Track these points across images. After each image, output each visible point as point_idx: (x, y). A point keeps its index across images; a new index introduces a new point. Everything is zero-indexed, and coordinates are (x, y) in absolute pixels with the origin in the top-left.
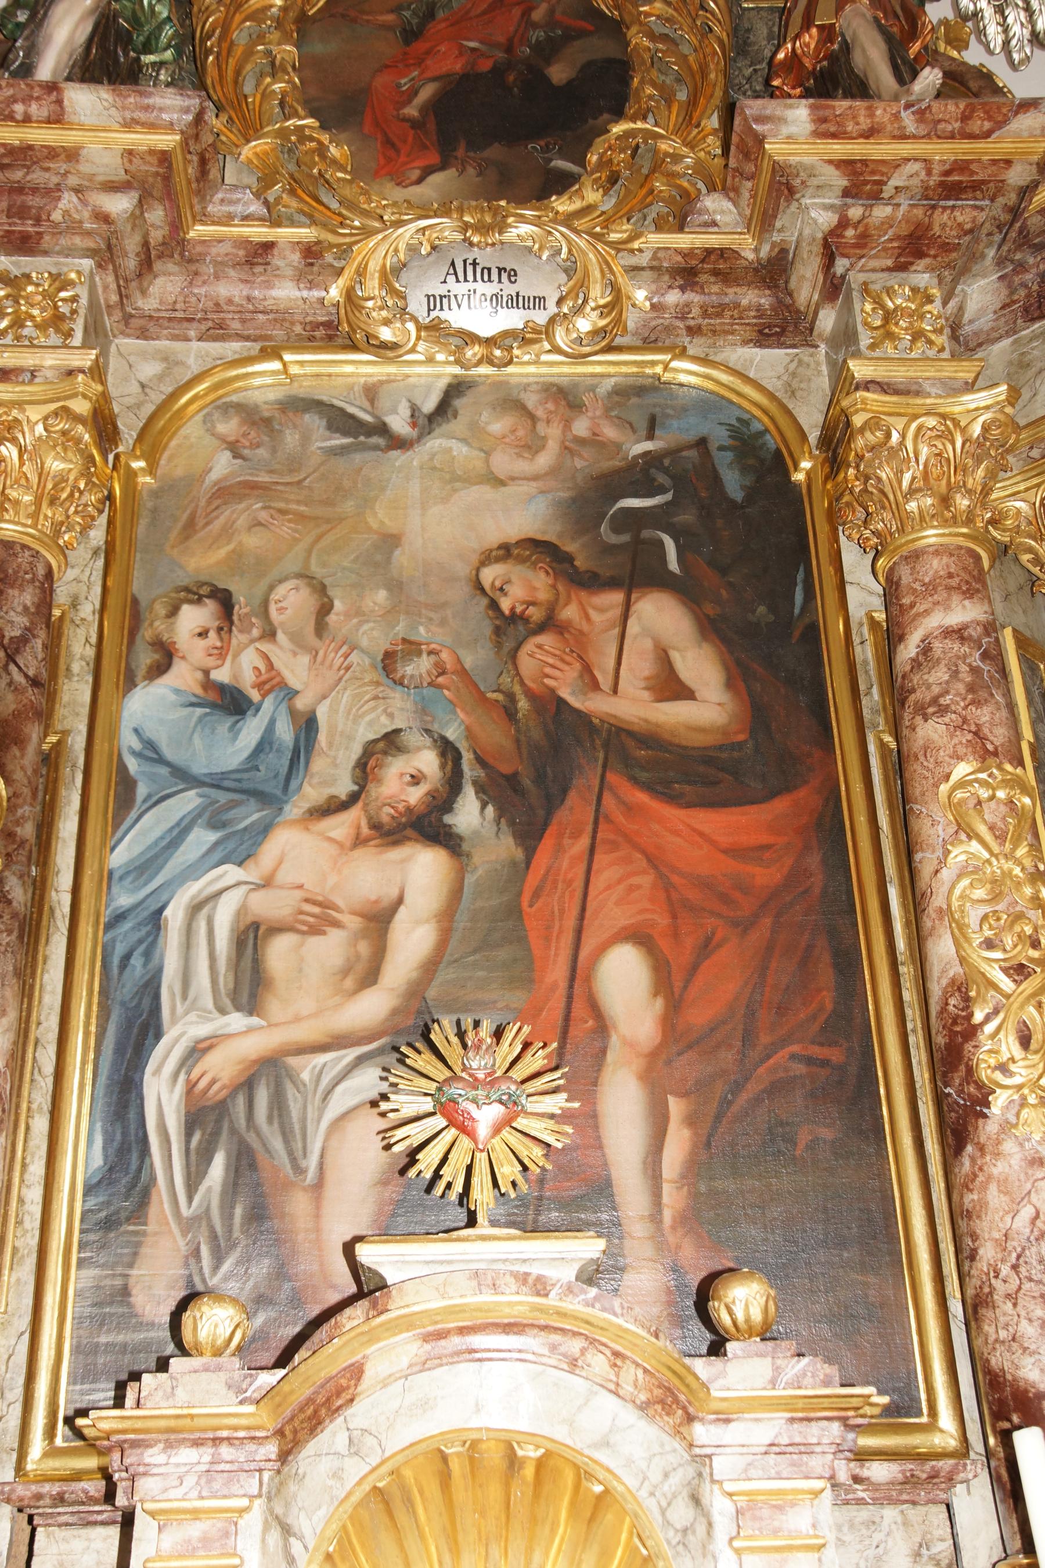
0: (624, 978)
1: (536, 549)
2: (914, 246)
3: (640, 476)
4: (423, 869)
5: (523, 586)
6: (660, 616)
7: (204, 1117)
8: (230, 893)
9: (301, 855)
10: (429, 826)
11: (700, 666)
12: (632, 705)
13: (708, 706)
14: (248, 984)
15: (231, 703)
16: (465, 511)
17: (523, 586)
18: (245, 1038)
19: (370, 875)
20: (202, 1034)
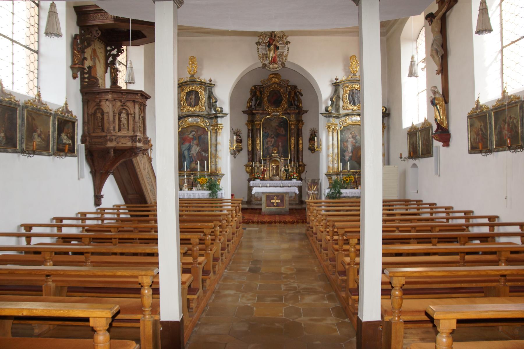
0: (280, 143)
1: (277, 126)
2: (293, 113)
3: (282, 122)
4: (273, 140)
5: (277, 127)
6: (282, 129)
7: (266, 148)
8: (266, 140)
9: (269, 139)
10: (273, 138)
11: (284, 131)
12: (281, 133)
13: (284, 133)
14: (267, 144)
15: (266, 133)
16: (275, 124)
17: (277, 127)
18: (267, 146)
19: (271, 140)
20: (266, 146)
